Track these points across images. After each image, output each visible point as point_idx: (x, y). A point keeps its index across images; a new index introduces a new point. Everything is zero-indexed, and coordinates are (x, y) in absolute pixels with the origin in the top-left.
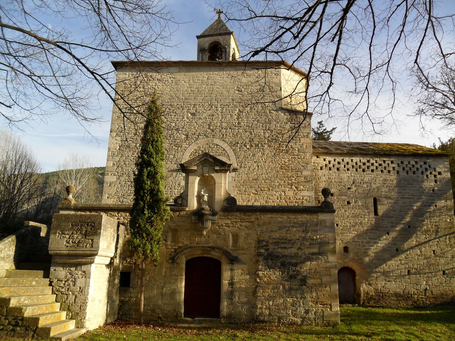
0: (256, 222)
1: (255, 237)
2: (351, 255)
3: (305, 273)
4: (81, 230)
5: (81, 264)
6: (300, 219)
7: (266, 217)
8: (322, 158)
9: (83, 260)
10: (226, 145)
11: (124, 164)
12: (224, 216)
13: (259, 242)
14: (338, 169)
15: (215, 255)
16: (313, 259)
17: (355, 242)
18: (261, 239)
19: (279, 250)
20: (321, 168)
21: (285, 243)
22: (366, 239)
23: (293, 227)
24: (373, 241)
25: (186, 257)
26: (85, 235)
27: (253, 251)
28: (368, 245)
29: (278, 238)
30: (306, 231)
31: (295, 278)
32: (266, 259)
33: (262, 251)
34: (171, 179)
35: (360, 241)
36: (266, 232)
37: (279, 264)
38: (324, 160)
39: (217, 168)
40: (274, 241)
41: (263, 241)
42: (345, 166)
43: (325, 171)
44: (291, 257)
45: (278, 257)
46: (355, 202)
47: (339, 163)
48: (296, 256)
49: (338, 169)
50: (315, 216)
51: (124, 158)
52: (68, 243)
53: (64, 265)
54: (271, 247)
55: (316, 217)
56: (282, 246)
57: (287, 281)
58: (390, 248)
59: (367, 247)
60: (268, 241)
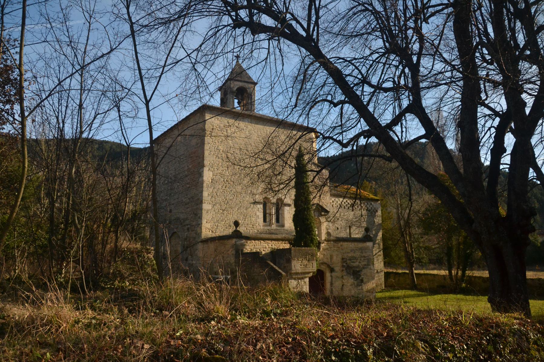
1: (340, 256)
3: (362, 277)
4: (306, 258)
5: (303, 278)
6: (359, 246)
7: (345, 244)
9: (307, 275)
11: (216, 195)
13: (343, 259)
15: (323, 268)
18: (343, 257)
19: (352, 264)
21: (353, 259)
23: (357, 250)
26: (309, 261)
27: (340, 264)
32: (346, 269)
33: (345, 264)
34: (250, 209)
36: (346, 253)
37: (352, 271)
39: (323, 213)
41: (344, 258)
45: (351, 268)
46: (341, 228)
47: (333, 202)
48: (358, 267)
50: (365, 244)
51: (216, 190)
52: (301, 265)
53: (295, 279)
54: (348, 262)
56: (353, 261)
57: (356, 281)
60: (346, 259)
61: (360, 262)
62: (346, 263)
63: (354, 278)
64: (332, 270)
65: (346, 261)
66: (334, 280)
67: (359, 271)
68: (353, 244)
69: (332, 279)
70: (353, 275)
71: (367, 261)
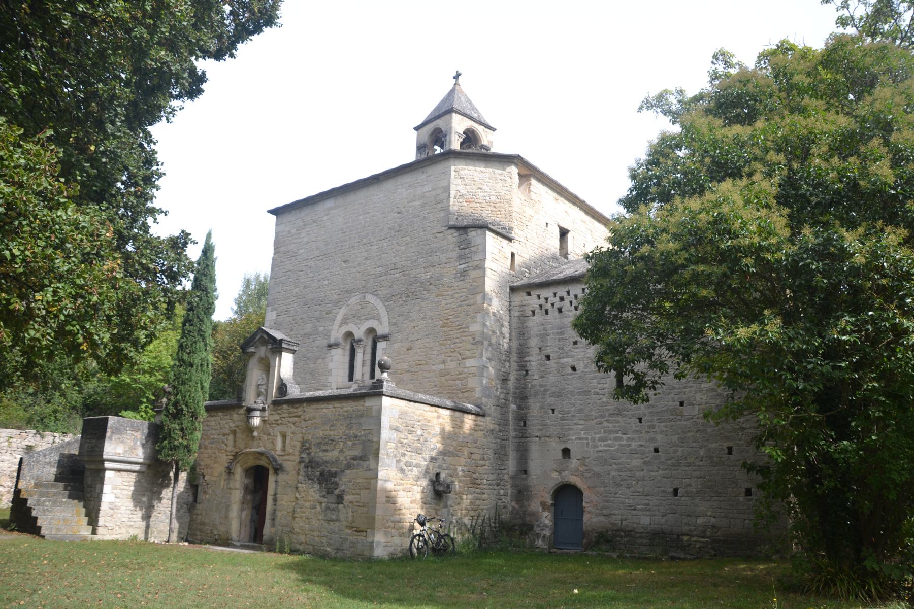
0: (302, 417)
2: (574, 463)
3: (343, 488)
6: (345, 409)
8: (534, 293)
10: (378, 301)
12: (275, 410)
13: (303, 443)
14: (560, 310)
15: (263, 462)
16: (354, 465)
17: (580, 439)
18: (305, 438)
20: (533, 312)
21: (326, 444)
22: (600, 433)
23: (337, 420)
24: (612, 436)
25: (241, 466)
28: (602, 443)
29: (322, 438)
30: (350, 427)
31: (332, 493)
32: (306, 467)
33: (304, 455)
35: (590, 437)
37: (318, 473)
38: (539, 297)
40: (318, 441)
42: (571, 302)
43: (539, 318)
44: (333, 463)
45: (318, 465)
47: (562, 299)
49: (560, 310)
50: (361, 403)
54: (314, 449)
55: (362, 403)
56: (324, 447)
57: (324, 496)
58: (643, 448)
59: (600, 448)
61: (341, 451)
62: (309, 454)
63: (320, 490)
64: (278, 470)
65: (308, 449)
66: (280, 490)
67: (335, 475)
68: (330, 406)
69: (276, 489)
70: (320, 483)
71: (360, 447)
